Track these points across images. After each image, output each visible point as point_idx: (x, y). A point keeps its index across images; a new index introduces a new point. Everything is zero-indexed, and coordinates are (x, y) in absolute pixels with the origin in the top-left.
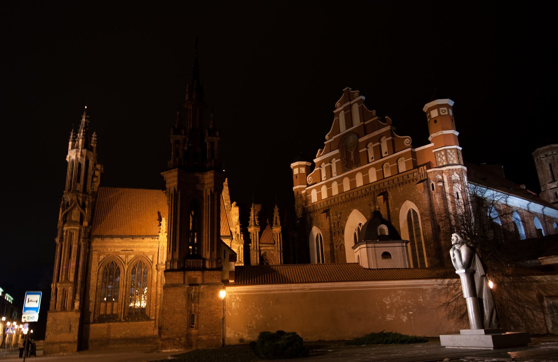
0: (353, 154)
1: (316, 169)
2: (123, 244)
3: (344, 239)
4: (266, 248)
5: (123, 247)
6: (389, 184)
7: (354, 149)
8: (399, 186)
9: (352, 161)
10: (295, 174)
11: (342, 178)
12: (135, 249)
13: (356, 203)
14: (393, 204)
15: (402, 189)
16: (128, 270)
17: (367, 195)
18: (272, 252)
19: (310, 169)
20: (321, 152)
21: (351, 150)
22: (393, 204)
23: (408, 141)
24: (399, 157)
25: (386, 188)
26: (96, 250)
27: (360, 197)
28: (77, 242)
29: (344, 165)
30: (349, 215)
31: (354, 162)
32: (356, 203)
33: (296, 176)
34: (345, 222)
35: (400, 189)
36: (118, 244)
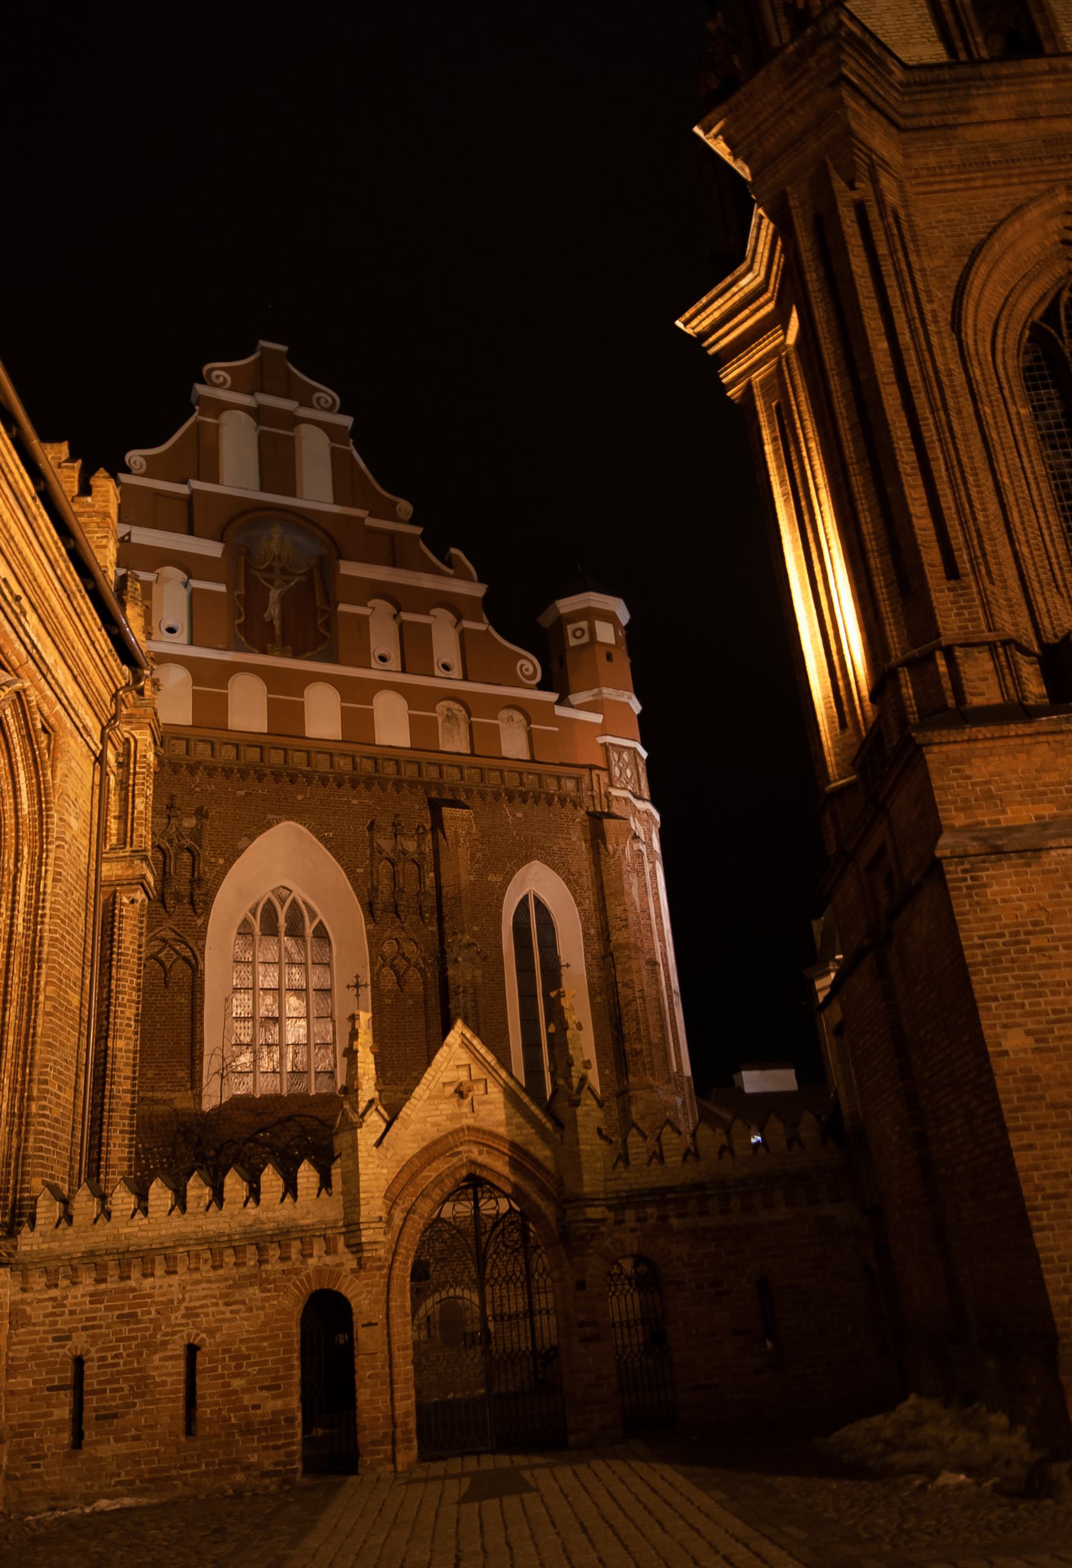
0: (283, 599)
3: (204, 938)
7: (288, 582)
8: (510, 800)
9: (271, 623)
13: (300, 797)
14: (479, 855)
15: (519, 815)
17: (362, 785)
21: (272, 582)
22: (479, 855)
23: (527, 670)
29: (237, 622)
30: (252, 838)
31: (278, 632)
32: (300, 797)
34: (221, 861)
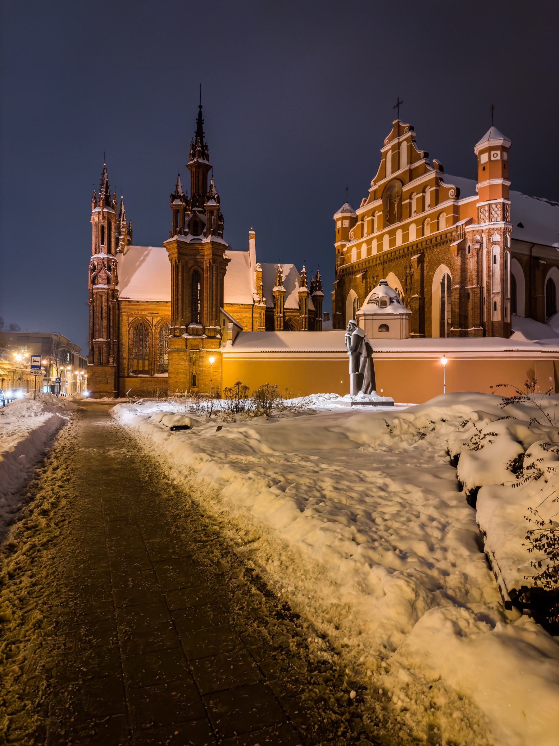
1: (359, 223)
2: (149, 307)
4: (290, 314)
5: (148, 309)
6: (426, 244)
10: (337, 227)
11: (383, 235)
12: (160, 312)
16: (155, 331)
18: (297, 318)
19: (353, 221)
20: (365, 201)
24: (440, 212)
25: (423, 250)
26: (125, 312)
27: (397, 258)
28: (106, 304)
33: (339, 231)
35: (437, 250)
36: (144, 307)
